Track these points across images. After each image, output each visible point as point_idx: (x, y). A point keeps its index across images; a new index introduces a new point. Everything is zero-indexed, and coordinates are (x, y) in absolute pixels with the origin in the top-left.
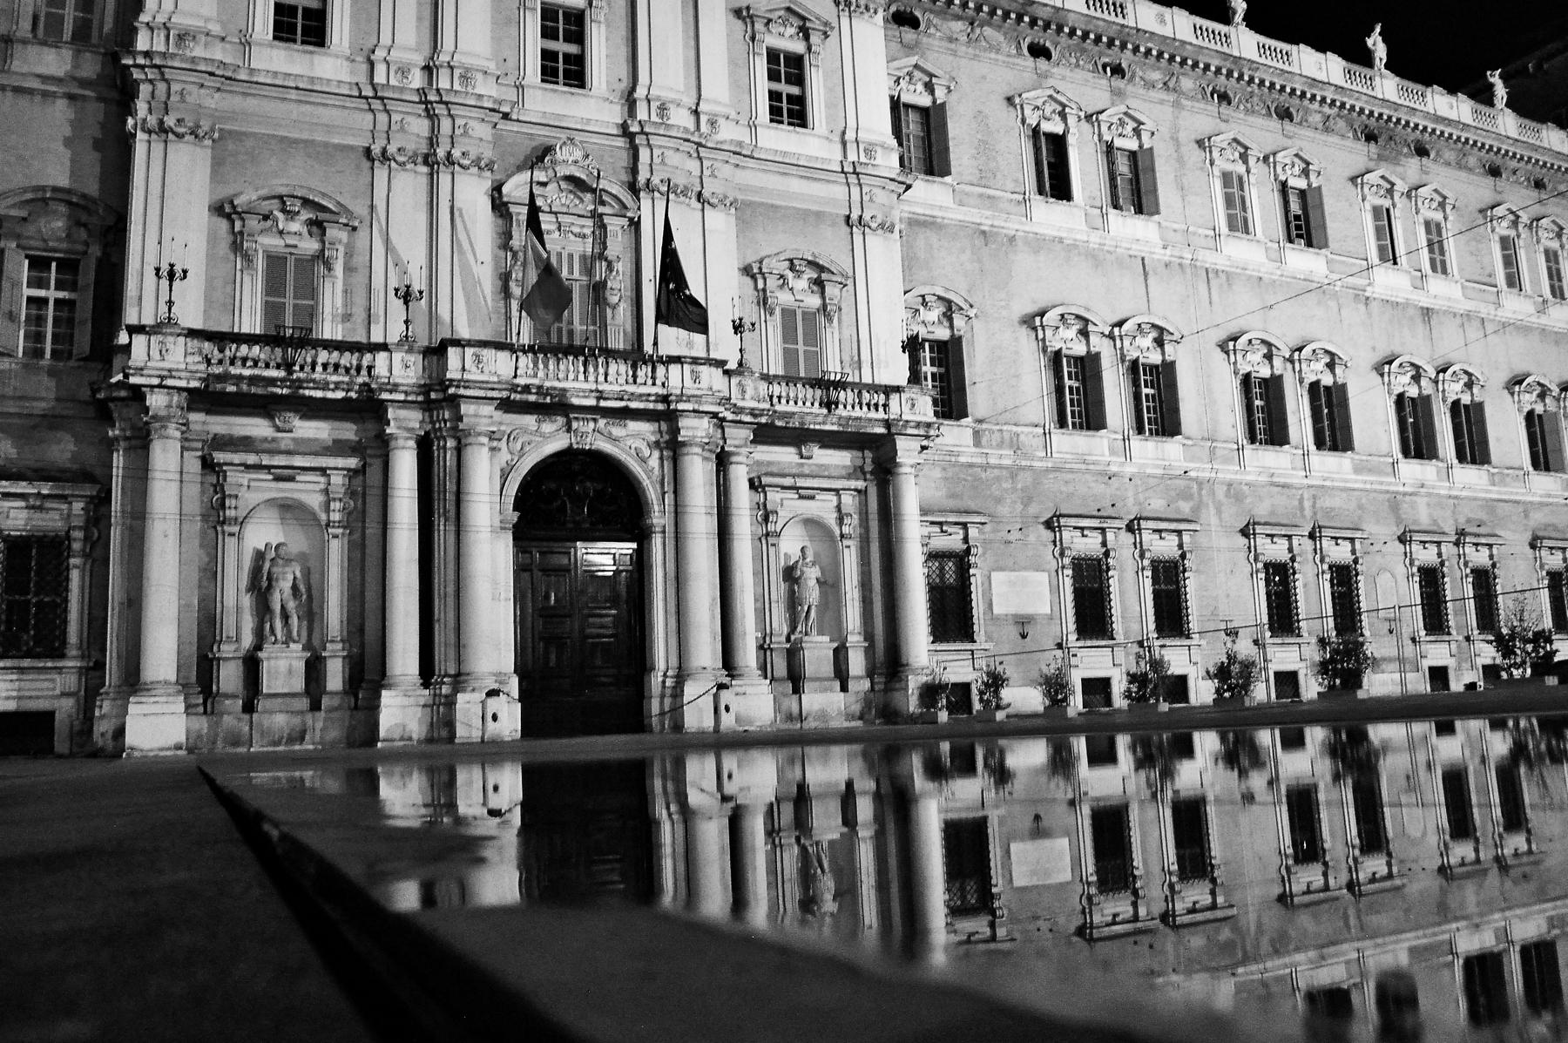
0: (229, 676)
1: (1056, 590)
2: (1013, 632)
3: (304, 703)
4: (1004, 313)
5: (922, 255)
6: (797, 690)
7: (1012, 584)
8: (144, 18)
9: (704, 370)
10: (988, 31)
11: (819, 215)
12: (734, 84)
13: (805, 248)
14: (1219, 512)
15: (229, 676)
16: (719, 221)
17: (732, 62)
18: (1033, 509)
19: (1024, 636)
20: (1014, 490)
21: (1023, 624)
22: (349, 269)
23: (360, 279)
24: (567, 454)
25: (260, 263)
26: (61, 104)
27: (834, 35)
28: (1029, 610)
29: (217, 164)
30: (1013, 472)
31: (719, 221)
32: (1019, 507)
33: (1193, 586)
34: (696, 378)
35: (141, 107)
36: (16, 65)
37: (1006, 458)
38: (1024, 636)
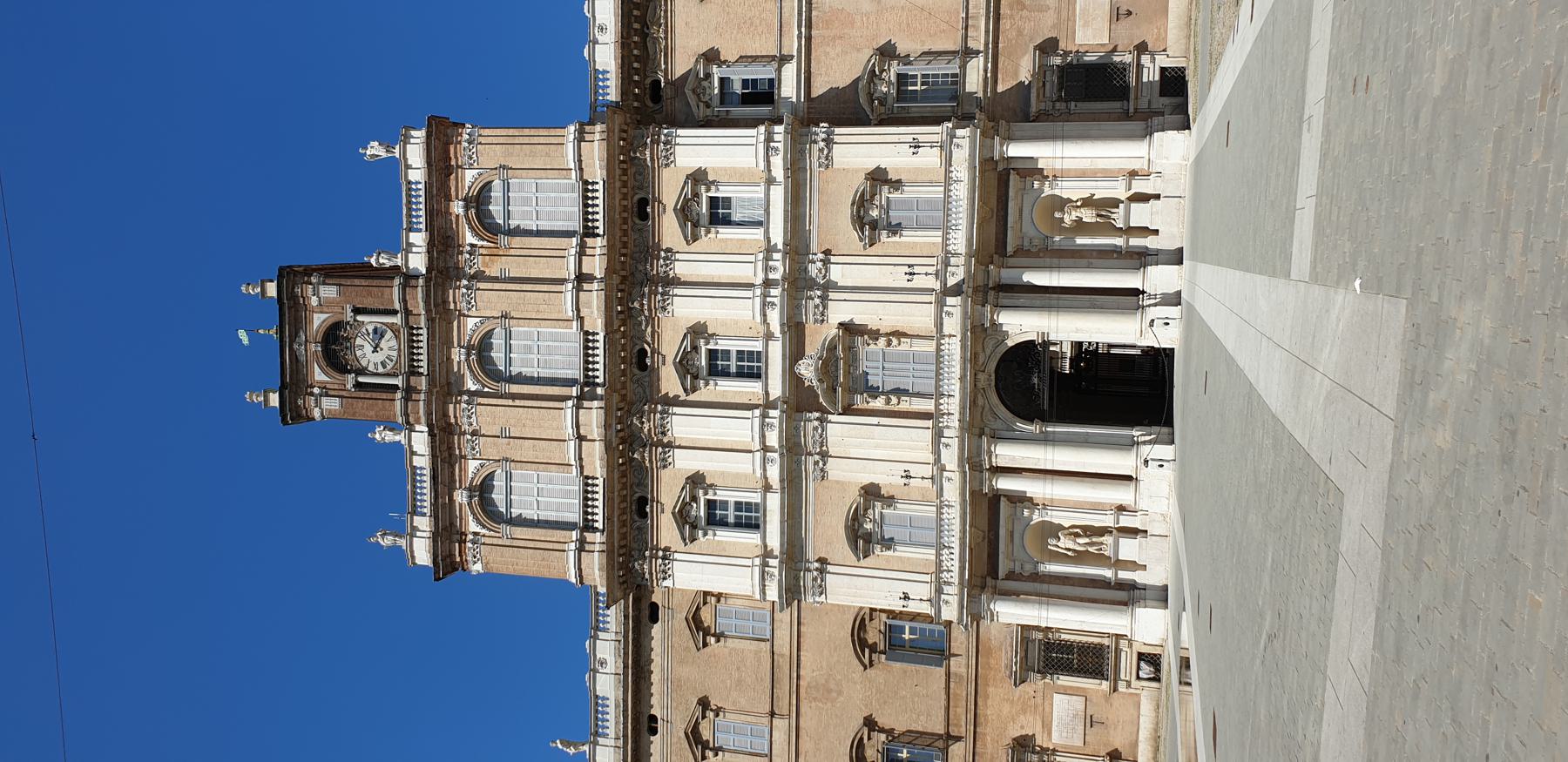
2: (1125, 23)
4: (872, 18)
7: (1086, 25)
19: (1129, 13)
28: (1108, 7)
32: (1025, 13)
38: (1129, 13)
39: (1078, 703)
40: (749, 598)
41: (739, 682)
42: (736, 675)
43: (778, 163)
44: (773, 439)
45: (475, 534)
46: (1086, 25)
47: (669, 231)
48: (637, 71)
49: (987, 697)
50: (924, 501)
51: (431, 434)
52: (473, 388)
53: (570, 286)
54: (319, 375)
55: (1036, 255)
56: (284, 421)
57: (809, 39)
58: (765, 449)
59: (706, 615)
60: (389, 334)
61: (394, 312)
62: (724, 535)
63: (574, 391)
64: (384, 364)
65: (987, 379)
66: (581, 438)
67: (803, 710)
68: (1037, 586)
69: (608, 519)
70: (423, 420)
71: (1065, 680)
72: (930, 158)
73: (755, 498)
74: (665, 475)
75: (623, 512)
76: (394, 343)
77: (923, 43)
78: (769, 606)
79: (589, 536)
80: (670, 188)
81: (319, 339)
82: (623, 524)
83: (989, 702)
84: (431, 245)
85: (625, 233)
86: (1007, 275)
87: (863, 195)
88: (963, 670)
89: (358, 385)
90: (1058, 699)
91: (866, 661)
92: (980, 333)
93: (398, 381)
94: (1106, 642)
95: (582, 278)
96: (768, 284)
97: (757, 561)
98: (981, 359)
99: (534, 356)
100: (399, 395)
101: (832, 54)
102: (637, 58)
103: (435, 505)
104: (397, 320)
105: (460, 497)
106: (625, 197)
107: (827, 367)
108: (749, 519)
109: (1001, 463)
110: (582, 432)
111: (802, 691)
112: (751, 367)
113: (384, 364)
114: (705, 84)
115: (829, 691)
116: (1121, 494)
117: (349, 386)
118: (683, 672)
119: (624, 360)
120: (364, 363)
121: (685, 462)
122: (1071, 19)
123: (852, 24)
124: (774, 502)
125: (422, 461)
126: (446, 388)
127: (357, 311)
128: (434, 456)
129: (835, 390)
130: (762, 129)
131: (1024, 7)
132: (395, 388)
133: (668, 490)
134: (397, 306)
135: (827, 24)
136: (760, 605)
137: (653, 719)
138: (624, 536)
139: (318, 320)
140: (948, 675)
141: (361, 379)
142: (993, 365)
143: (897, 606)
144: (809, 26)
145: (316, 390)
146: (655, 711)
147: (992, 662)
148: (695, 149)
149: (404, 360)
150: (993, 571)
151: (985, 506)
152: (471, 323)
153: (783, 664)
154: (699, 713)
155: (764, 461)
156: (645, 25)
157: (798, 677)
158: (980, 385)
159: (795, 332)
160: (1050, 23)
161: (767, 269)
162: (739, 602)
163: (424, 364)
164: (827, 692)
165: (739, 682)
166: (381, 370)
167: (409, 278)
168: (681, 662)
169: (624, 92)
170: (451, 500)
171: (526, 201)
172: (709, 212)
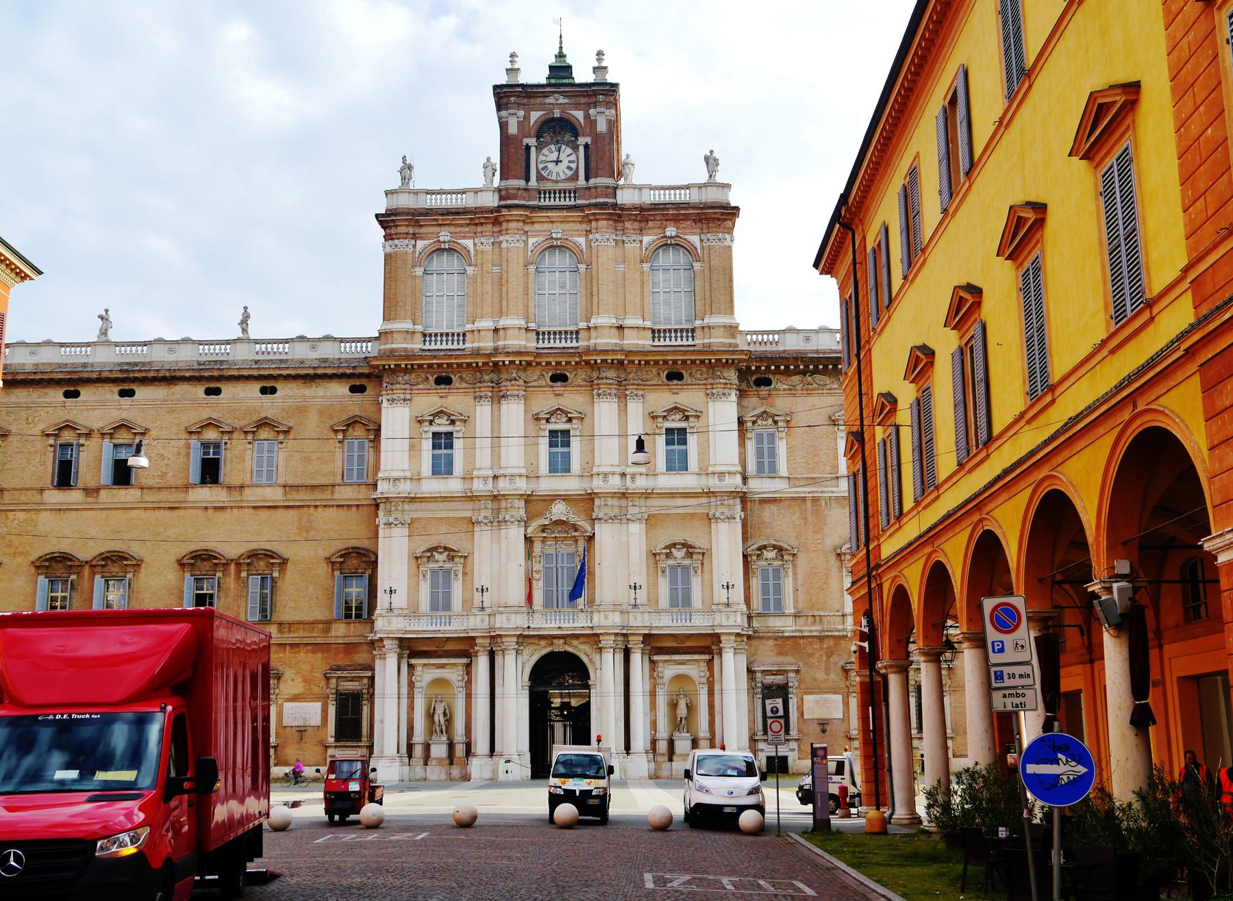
0: (418, 751)
1: (846, 704)
2: (818, 729)
3: (447, 761)
4: (820, 547)
5: (767, 520)
6: (671, 760)
8: (380, 475)
9: (610, 615)
10: (817, 377)
11: (692, 515)
15: (418, 751)
18: (834, 659)
19: (824, 731)
20: (822, 649)
21: (823, 725)
22: (464, 574)
23: (468, 577)
24: (552, 654)
25: (428, 576)
26: (354, 509)
28: (829, 716)
30: (821, 639)
31: (636, 529)
32: (824, 658)
34: (606, 618)
35: (381, 513)
36: (337, 496)
37: (815, 630)
38: (824, 731)
39: (316, 720)
40: (377, 468)
42: (314, 456)
43: (713, 483)
44: (504, 486)
45: (414, 246)
46: (817, 702)
48: (778, 367)
49: (314, 652)
50: (464, 602)
52: (531, 241)
53: (614, 321)
54: (535, 116)
55: (651, 677)
56: (495, 87)
58: (495, 477)
59: (359, 432)
60: (569, 173)
61: (587, 179)
62: (427, 444)
63: (532, 326)
64: (545, 168)
65: (559, 646)
67: (291, 512)
68: (405, 690)
69: (434, 354)
70: (503, 203)
71: (332, 710)
72: (721, 596)
74: (469, 399)
75: (440, 365)
76: (563, 177)
77: (803, 585)
78: (370, 481)
79: (419, 337)
80: (689, 397)
81: (566, 116)
82: (430, 366)
83: (310, 655)
85: (656, 362)
86: (636, 658)
87: (692, 547)
88: (333, 634)
89: (528, 148)
90: (318, 706)
91: (333, 560)
92: (594, 639)
93: (533, 182)
94: (364, 739)
97: (408, 474)
98: (575, 642)
99: (557, 291)
100: (522, 183)
101: (794, 518)
102: (787, 367)
104: (582, 182)
105: (445, 235)
106: (684, 362)
107: (560, 522)
108: (442, 468)
109: (498, 659)
110: (501, 332)
111: (305, 510)
113: (545, 168)
114: (770, 421)
115: (307, 531)
116: (481, 745)
117: (526, 141)
118: (313, 416)
119: (558, 363)
120: (545, 151)
121: (483, 413)
123: (815, 532)
124: (453, 485)
127: (586, 146)
129: (543, 531)
130: (739, 469)
131: (829, 657)
132: (528, 180)
133: (456, 400)
134: (592, 181)
136: (370, 474)
138: (420, 366)
139: (579, 115)
141: (533, 150)
142: (570, 649)
143: (382, 584)
145: (521, 113)
147: (341, 656)
148: (723, 412)
149: (549, 186)
150: (414, 654)
152: (581, 240)
153: (326, 495)
154: (282, 428)
155: (485, 478)
157: (316, 507)
158: (555, 641)
159: (589, 498)
160: (818, 676)
161: (633, 476)
162: (371, 458)
163: (547, 203)
165: (308, 460)
166: (541, 166)
167: (616, 188)
171: (677, 285)
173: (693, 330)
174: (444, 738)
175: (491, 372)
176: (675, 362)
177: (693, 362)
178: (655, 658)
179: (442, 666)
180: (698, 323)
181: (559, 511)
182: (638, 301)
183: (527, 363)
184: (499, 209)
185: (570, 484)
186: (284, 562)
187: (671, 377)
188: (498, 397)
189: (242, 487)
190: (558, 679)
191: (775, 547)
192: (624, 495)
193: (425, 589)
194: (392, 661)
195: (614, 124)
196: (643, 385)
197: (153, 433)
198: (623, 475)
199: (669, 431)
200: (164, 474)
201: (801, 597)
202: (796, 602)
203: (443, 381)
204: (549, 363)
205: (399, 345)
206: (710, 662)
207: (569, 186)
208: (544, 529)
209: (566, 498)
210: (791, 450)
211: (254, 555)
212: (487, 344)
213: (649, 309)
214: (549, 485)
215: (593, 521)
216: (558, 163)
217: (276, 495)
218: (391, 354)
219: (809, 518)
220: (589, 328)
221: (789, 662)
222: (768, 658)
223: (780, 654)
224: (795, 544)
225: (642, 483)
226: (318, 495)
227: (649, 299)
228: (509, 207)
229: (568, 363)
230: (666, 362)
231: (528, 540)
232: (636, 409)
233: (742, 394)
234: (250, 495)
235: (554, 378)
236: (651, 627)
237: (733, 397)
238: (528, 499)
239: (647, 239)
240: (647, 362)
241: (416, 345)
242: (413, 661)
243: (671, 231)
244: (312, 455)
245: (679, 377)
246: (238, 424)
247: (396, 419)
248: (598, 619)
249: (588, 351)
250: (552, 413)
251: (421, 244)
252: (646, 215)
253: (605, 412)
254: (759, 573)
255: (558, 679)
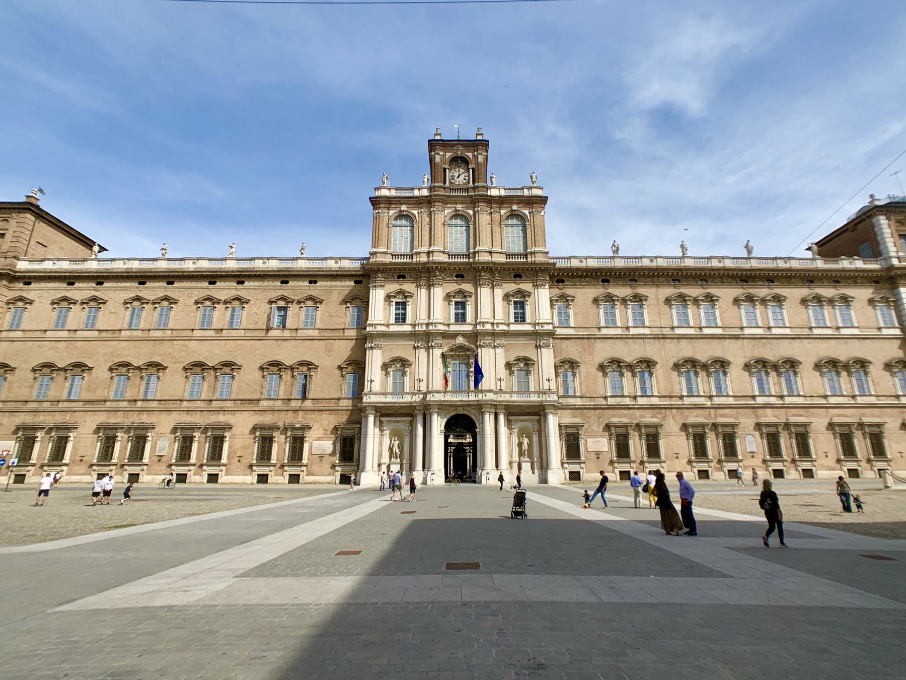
12: (504, 313)
13: (522, 354)
14: (674, 417)
16: (498, 350)
17: (504, 307)
27: (532, 296)
29: (383, 352)
33: (662, 443)
40: (367, 319)
41: (332, 316)
47: (511, 287)
51: (427, 197)
52: (446, 211)
57: (583, 338)
66: (428, 253)
69: (397, 264)
73: (409, 320)
75: (400, 269)
82: (395, 269)
84: (500, 197)
93: (448, 184)
95: (491, 253)
96: (493, 324)
103: (400, 197)
104: (471, 184)
105: (404, 208)
106: (523, 269)
107: (461, 348)
108: (401, 318)
112: (461, 318)
119: (460, 269)
122: (595, 437)
124: (407, 328)
125: (417, 193)
126: (445, 201)
127: (473, 169)
128: (418, 197)
132: (445, 183)
133: (408, 287)
135: (589, 345)
137: (315, 282)
138: (390, 269)
140: (339, 399)
144: (588, 338)
146: (319, 283)
149: (455, 187)
150: (382, 415)
151: (408, 411)
152: (471, 212)
153: (341, 333)
155: (422, 324)
156: (585, 277)
161: (498, 324)
164: (329, 351)
165: (332, 316)
168: (339, 293)
169: (560, 269)
170: (402, 204)
172: (519, 302)
173: (526, 255)
174: (398, 460)
175: (426, 273)
176: (518, 269)
177: (527, 269)
178: (511, 418)
179: (398, 422)
180: (529, 250)
181: (460, 340)
182: (500, 241)
183: (443, 268)
184: (430, 196)
185: (468, 328)
186: (317, 367)
187: (515, 276)
188: (429, 287)
189: (297, 329)
190: (462, 423)
191: (569, 362)
192: (494, 335)
193: (390, 380)
194: (371, 419)
195: (486, 159)
196: (504, 279)
197: (252, 302)
198: (493, 324)
199: (515, 303)
200: (257, 323)
201: (583, 388)
202: (581, 390)
203: (402, 277)
204: (455, 269)
205: (380, 259)
206: (539, 421)
207: (464, 187)
208: (452, 350)
209: (464, 335)
210: (575, 314)
211: (301, 364)
212: (424, 259)
213: (505, 244)
214: (454, 328)
215: (477, 347)
216: (460, 177)
217: (315, 333)
218: (376, 264)
219: (586, 347)
220: (475, 253)
221: (577, 420)
222: (568, 419)
223: (574, 417)
224: (579, 360)
225: (502, 327)
226: (336, 334)
227: (504, 240)
228: (435, 195)
229: (465, 269)
230: (513, 269)
231: (443, 356)
232: (499, 293)
233: (551, 287)
234: (300, 333)
235: (457, 276)
236: (509, 402)
237: (547, 286)
238: (445, 335)
239: (503, 212)
240: (504, 269)
241: (388, 259)
242: (382, 419)
243: (515, 207)
244: (335, 313)
245: (520, 276)
246: (296, 298)
247: (377, 296)
248: (480, 397)
249: (474, 263)
250: (456, 293)
251: (391, 212)
252: (501, 201)
253: (484, 292)
254: (561, 374)
255: (462, 423)
